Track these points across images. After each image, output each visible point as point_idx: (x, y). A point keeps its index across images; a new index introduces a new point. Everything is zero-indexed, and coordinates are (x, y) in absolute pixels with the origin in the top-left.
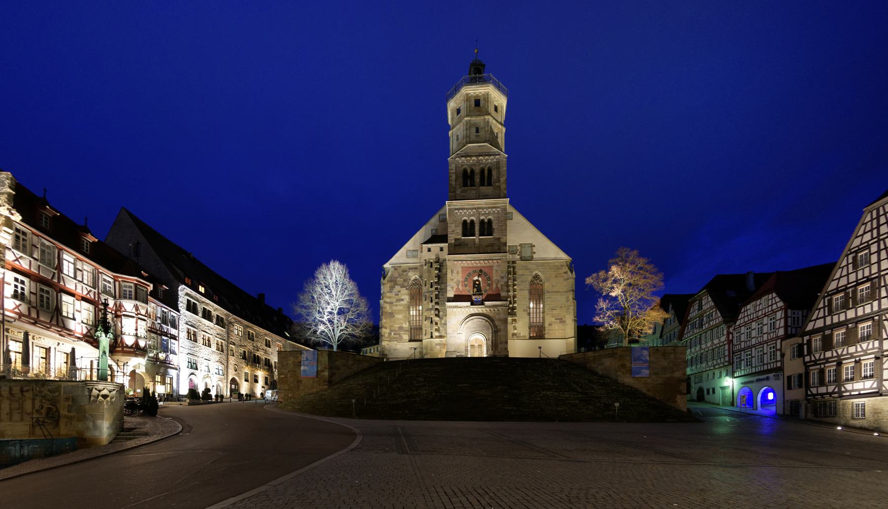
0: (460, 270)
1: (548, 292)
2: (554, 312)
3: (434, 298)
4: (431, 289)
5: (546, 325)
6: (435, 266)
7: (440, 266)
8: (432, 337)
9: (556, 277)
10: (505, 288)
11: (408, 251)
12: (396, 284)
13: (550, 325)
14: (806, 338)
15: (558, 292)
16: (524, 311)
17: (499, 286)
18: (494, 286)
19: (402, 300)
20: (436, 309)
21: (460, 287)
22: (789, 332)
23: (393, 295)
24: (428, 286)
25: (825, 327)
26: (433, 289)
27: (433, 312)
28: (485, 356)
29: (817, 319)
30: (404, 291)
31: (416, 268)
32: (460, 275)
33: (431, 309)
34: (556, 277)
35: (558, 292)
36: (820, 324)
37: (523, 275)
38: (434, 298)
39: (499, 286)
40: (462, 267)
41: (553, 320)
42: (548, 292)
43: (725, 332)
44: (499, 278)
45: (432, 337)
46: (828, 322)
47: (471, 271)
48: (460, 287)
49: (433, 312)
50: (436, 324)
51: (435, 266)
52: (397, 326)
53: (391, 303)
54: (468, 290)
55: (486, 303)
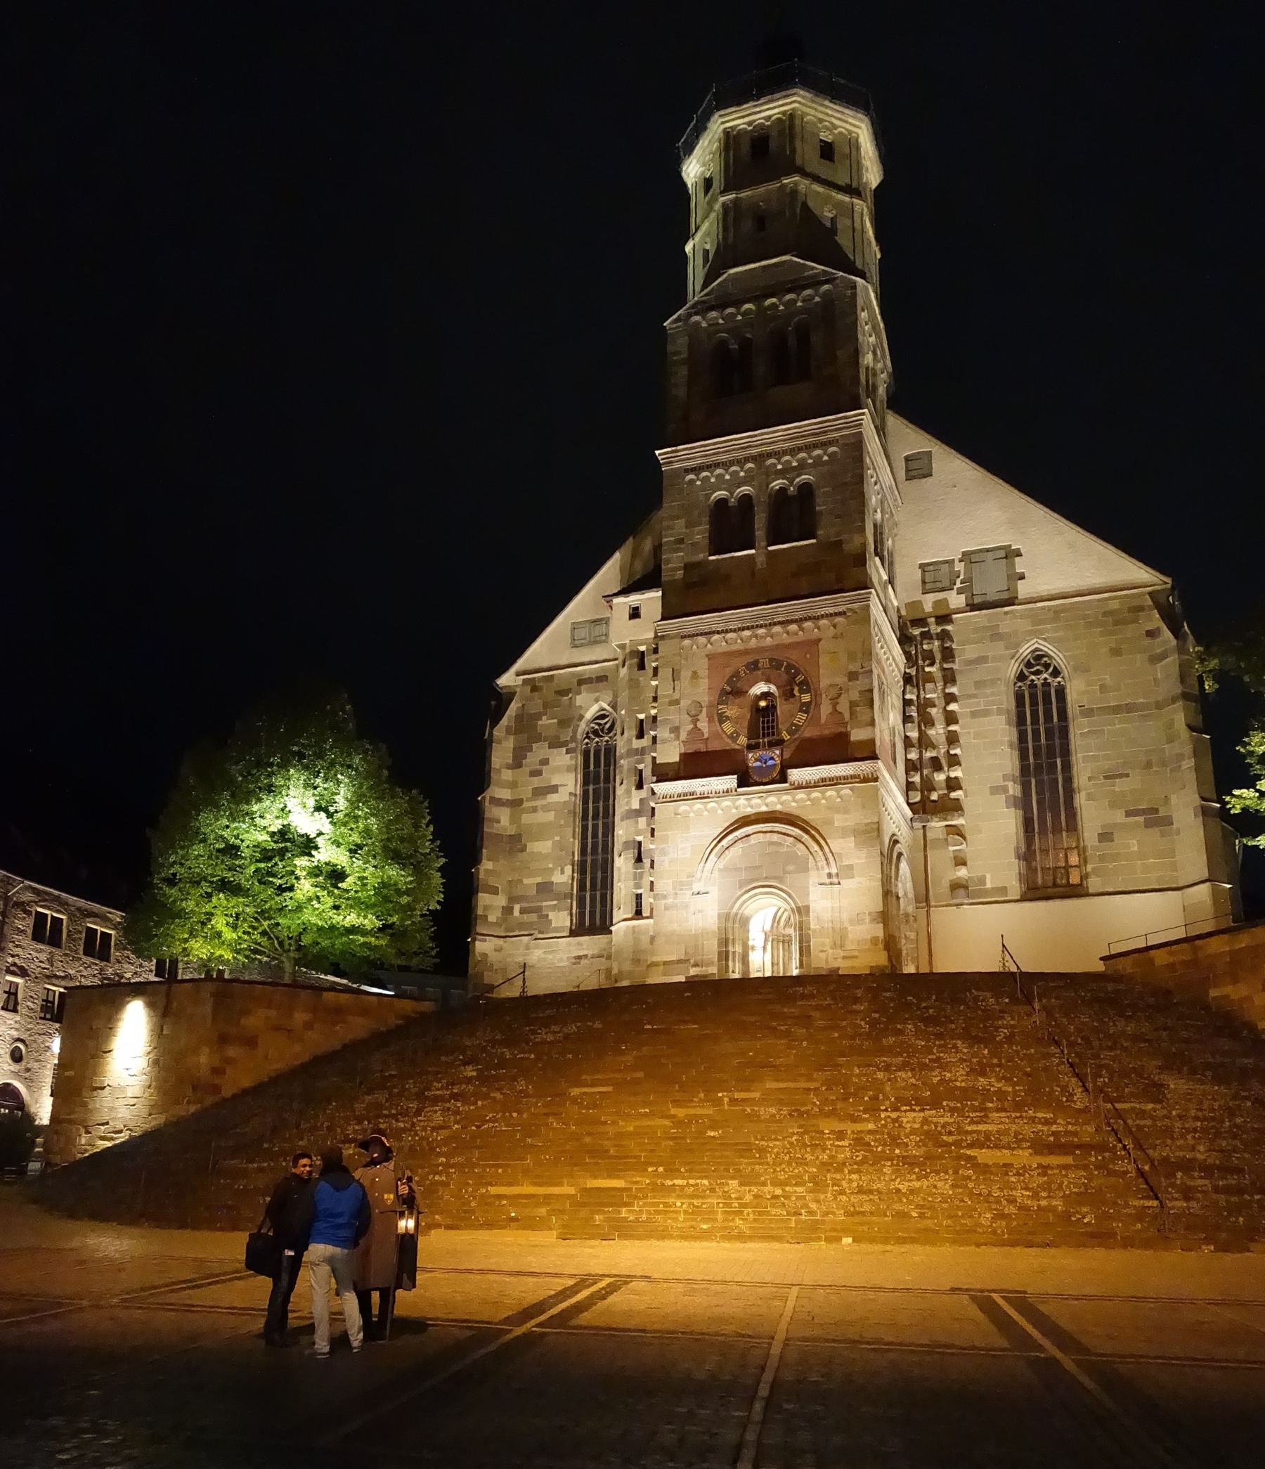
0: (703, 666)
1: (1088, 713)
4: (637, 744)
8: (638, 914)
9: (1116, 652)
16: (995, 790)
17: (843, 707)
18: (825, 710)
21: (703, 725)
24: (631, 732)
28: (795, 972)
31: (602, 678)
32: (704, 683)
34: (1116, 652)
37: (982, 660)
39: (843, 707)
40: (710, 657)
42: (1088, 713)
44: (841, 680)
47: (740, 663)
48: (703, 725)
52: (531, 881)
54: (731, 732)
55: (796, 774)
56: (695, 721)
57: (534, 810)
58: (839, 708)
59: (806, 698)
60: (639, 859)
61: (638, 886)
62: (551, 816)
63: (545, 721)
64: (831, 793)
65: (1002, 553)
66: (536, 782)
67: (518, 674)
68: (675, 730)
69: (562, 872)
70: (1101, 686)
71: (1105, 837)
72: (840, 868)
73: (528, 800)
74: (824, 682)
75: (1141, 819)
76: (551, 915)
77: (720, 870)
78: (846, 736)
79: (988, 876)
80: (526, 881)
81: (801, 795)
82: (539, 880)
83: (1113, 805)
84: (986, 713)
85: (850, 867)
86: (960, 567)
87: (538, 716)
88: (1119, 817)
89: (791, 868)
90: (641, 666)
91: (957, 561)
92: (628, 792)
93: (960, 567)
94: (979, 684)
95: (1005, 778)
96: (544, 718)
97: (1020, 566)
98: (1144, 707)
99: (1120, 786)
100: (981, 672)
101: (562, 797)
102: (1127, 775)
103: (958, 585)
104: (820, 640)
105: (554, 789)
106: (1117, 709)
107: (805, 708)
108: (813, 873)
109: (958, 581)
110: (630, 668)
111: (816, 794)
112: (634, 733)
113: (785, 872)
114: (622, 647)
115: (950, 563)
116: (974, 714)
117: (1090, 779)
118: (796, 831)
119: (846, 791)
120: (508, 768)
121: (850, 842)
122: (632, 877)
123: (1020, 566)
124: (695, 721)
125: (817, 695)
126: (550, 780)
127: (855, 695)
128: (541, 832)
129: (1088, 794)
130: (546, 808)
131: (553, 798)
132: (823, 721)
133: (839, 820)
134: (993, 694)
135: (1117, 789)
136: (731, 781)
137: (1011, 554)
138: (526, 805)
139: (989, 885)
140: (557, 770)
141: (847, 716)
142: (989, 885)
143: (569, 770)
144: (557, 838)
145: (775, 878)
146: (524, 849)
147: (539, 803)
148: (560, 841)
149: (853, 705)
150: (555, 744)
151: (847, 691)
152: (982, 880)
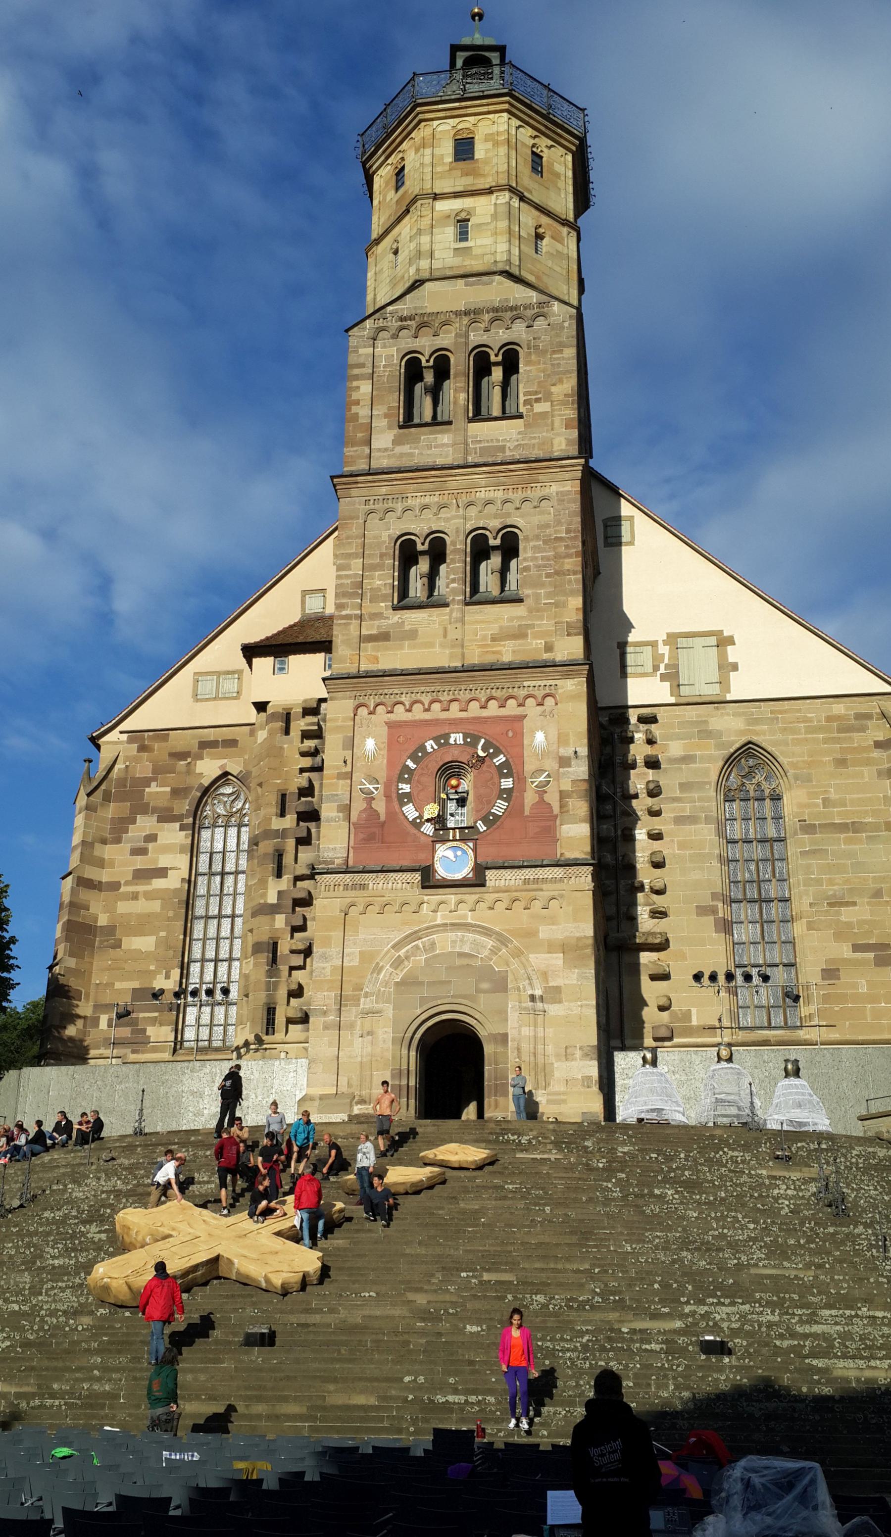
1: (808, 828)
11: (198, 676)
12: (144, 809)
15: (855, 827)
16: (702, 910)
18: (530, 798)
21: (380, 806)
26: (289, 821)
27: (280, 921)
31: (232, 743)
33: (274, 909)
34: (841, 763)
35: (855, 827)
37: (687, 759)
39: (552, 798)
42: (808, 828)
44: (551, 765)
48: (380, 806)
51: (300, 724)
57: (135, 896)
58: (547, 798)
59: (507, 783)
62: (155, 906)
63: (154, 788)
65: (713, 640)
66: (140, 862)
67: (121, 732)
68: (346, 809)
69: (167, 977)
70: (824, 800)
71: (830, 973)
72: (547, 989)
73: (127, 883)
74: (529, 766)
75: (871, 955)
76: (151, 1031)
77: (397, 983)
79: (694, 1011)
80: (118, 985)
82: (136, 985)
83: (839, 936)
84: (692, 819)
85: (558, 989)
86: (664, 650)
87: (147, 782)
88: (845, 951)
89: (485, 986)
90: (287, 732)
91: (660, 643)
92: (263, 883)
93: (664, 650)
94: (684, 787)
95: (714, 896)
96: (153, 784)
97: (733, 654)
98: (876, 827)
99: (846, 915)
100: (685, 773)
101: (174, 882)
102: (854, 904)
103: (662, 670)
104: (525, 716)
105: (162, 873)
106: (843, 827)
108: (512, 996)
109: (662, 666)
110: (271, 733)
112: (274, 809)
113: (478, 991)
114: (261, 707)
115: (654, 644)
116: (679, 820)
117: (811, 904)
118: (489, 943)
120: (104, 842)
121: (558, 959)
122: (263, 986)
123: (733, 654)
125: (520, 781)
126: (156, 860)
127: (566, 786)
128: (142, 925)
129: (809, 923)
130: (149, 896)
131: (158, 883)
132: (527, 812)
134: (700, 799)
135: (843, 918)
137: (724, 642)
138: (123, 889)
139: (695, 1022)
140: (167, 849)
141: (556, 810)
142: (695, 1022)
143: (182, 851)
144: (163, 934)
145: (464, 997)
146: (118, 945)
147: (141, 888)
148: (167, 938)
149: (563, 795)
150: (166, 816)
151: (558, 779)
152: (687, 1015)
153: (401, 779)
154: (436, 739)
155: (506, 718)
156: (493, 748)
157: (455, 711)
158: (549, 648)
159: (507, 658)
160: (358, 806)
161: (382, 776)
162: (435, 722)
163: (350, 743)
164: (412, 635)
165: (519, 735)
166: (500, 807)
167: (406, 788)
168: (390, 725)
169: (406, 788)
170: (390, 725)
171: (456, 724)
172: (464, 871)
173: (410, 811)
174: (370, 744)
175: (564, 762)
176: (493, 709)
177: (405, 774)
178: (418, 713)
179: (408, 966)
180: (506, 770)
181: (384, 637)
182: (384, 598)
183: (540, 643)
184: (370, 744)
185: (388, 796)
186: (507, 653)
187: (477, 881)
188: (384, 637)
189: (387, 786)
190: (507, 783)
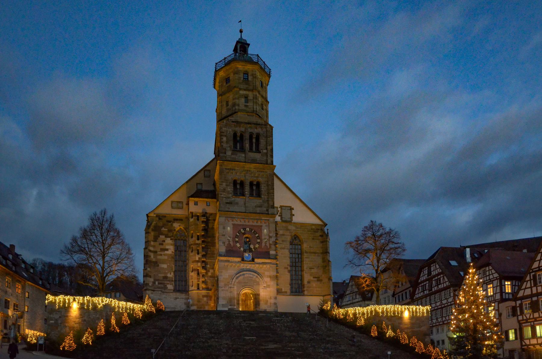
2: (313, 271)
3: (200, 250)
5: (305, 282)
6: (203, 219)
7: (207, 220)
8: (198, 289)
10: (273, 247)
13: (309, 282)
14: (518, 302)
17: (268, 245)
18: (263, 244)
19: (167, 250)
20: (203, 262)
21: (231, 243)
22: (504, 297)
23: (157, 244)
25: (532, 296)
28: (252, 310)
29: (526, 288)
30: (168, 241)
36: (528, 292)
38: (200, 250)
39: (268, 245)
41: (312, 278)
43: (452, 294)
44: (268, 237)
45: (198, 289)
46: (534, 291)
48: (231, 243)
49: (199, 264)
50: (203, 276)
53: (155, 252)
55: (256, 260)
56: (229, 241)
59: (259, 241)
60: (198, 274)
61: (198, 281)
64: (265, 266)
68: (224, 243)
74: (263, 238)
78: (269, 252)
81: (257, 266)
85: (269, 285)
107: (259, 243)
111: (261, 266)
118: (256, 275)
119: (268, 266)
121: (269, 279)
124: (229, 241)
127: (271, 242)
133: (267, 273)
136: (239, 259)
149: (270, 244)
153: (236, 237)
154: (243, 229)
155: (258, 226)
156: (255, 233)
157: (247, 223)
158: (267, 210)
159: (258, 212)
160: (227, 243)
161: (232, 236)
162: (243, 225)
163: (224, 228)
164: (237, 203)
165: (261, 230)
166: (257, 246)
167: (237, 239)
168: (234, 225)
169: (237, 239)
170: (234, 225)
171: (248, 226)
172: (251, 259)
173: (238, 245)
174: (229, 228)
175: (270, 237)
176: (255, 224)
177: (237, 236)
178: (239, 223)
179: (240, 278)
180: (259, 237)
181: (230, 203)
182: (231, 194)
183: (265, 209)
184: (229, 228)
185: (233, 241)
186: (258, 210)
187: (253, 260)
188: (230, 203)
189: (233, 238)
190: (259, 241)
